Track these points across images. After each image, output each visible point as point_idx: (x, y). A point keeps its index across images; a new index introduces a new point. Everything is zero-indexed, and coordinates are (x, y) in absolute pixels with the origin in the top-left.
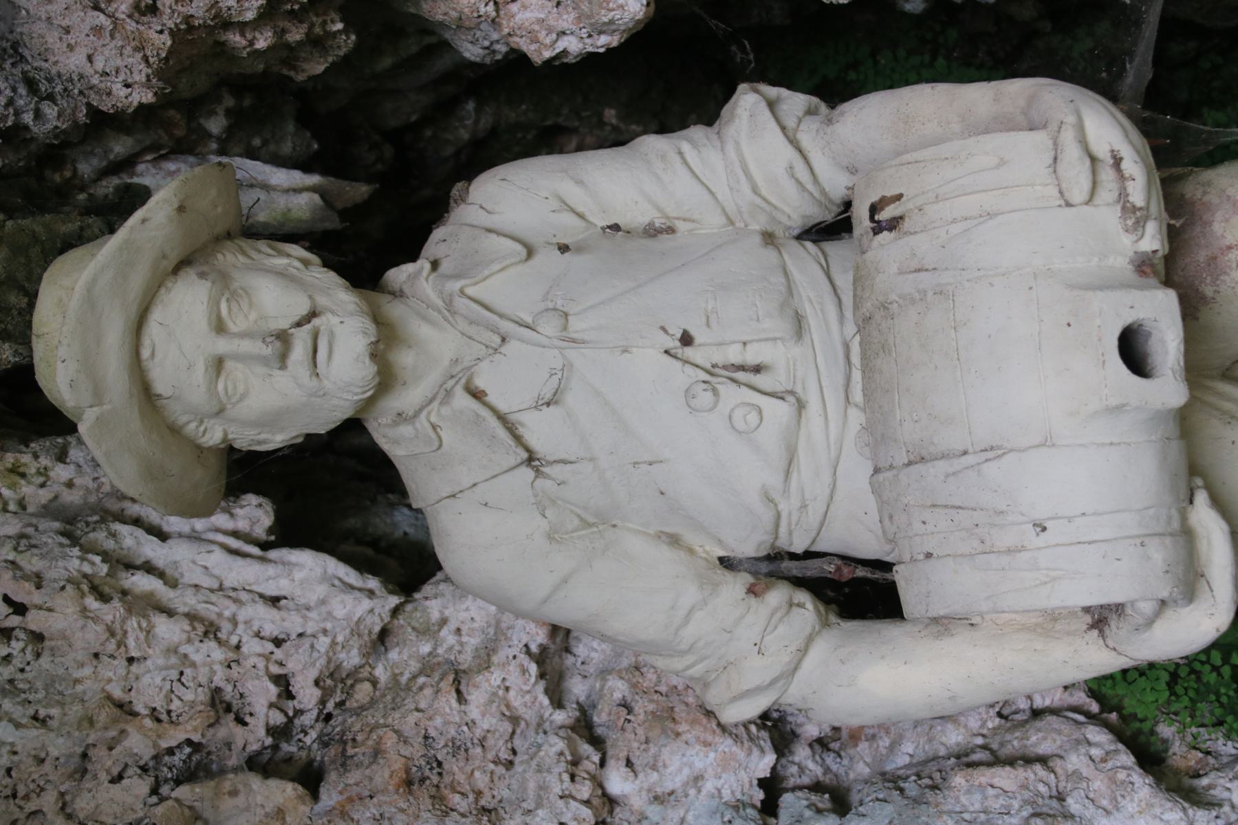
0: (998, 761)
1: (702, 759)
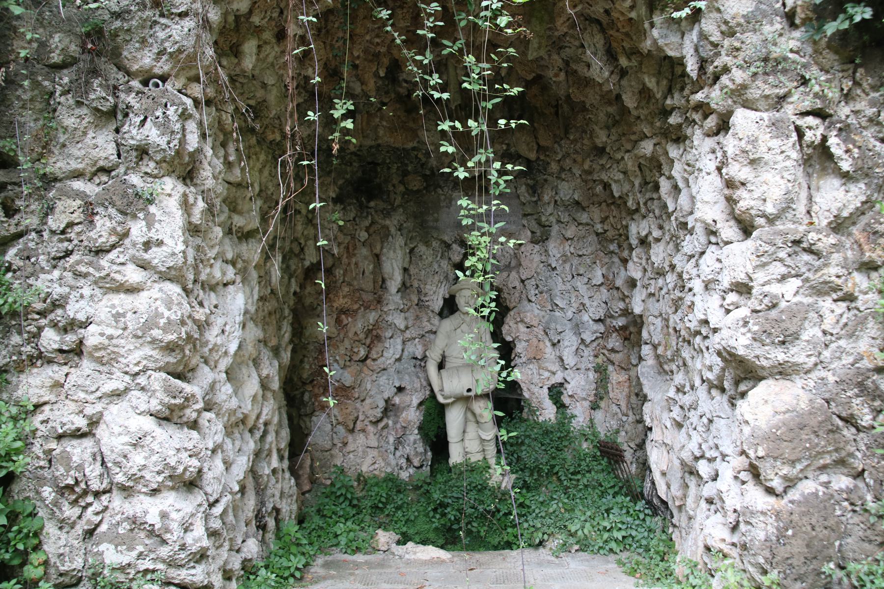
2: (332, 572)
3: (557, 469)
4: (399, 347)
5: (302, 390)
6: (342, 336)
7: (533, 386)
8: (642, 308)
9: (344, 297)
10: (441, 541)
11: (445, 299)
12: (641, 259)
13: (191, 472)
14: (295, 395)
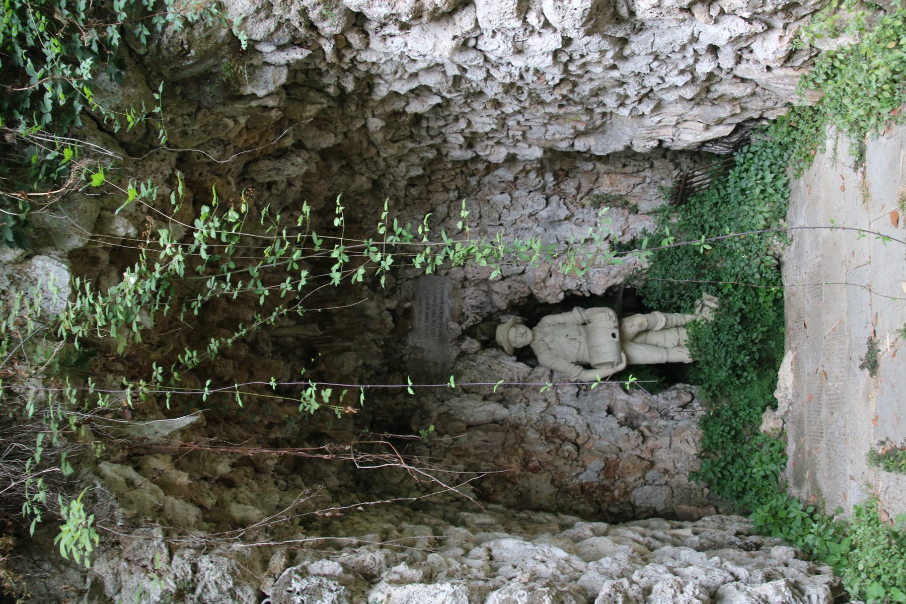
1: (569, 389)
2: (807, 475)
4: (566, 409)
5: (606, 514)
7: (612, 272)
8: (537, 148)
9: (510, 462)
10: (772, 371)
11: (518, 361)
12: (487, 146)
13: (700, 592)
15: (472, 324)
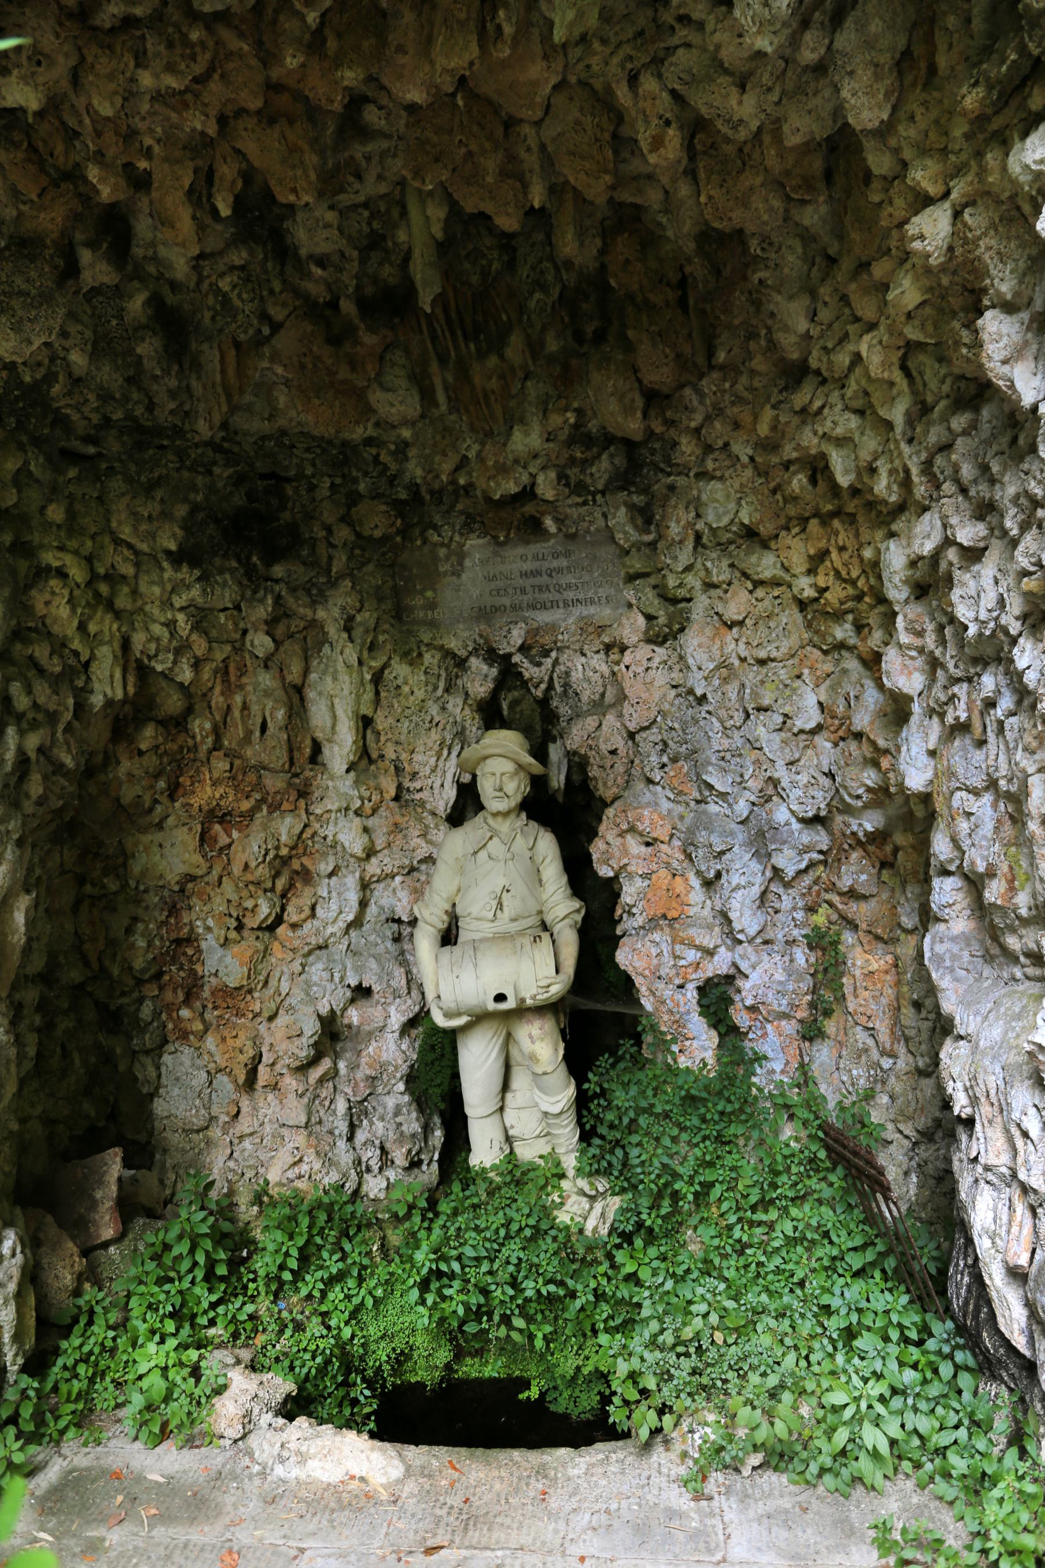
0: (408, 982)
1: (405, 901)
3: (717, 1191)
4: (353, 897)
5: (136, 995)
6: (215, 873)
7: (660, 985)
8: (929, 774)
9: (215, 784)
12: (920, 634)
14: (121, 1007)
15: (527, 675)
